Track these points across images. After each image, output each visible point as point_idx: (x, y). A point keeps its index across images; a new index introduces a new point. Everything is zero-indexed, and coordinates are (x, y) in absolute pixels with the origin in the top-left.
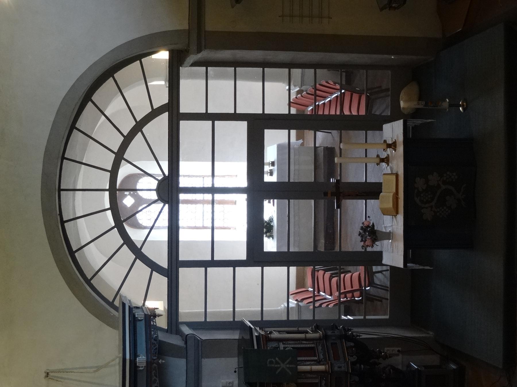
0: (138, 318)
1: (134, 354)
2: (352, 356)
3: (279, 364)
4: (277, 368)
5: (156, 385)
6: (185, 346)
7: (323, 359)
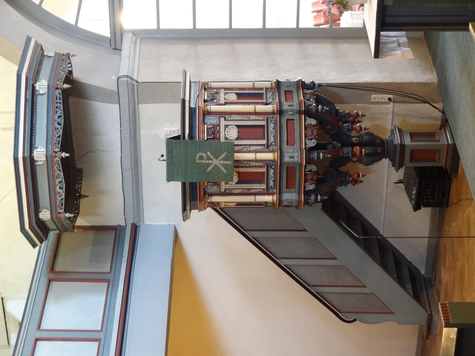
0: (39, 91)
1: (32, 147)
2: (311, 140)
3: (211, 159)
4: (209, 165)
5: (60, 180)
7: (273, 142)
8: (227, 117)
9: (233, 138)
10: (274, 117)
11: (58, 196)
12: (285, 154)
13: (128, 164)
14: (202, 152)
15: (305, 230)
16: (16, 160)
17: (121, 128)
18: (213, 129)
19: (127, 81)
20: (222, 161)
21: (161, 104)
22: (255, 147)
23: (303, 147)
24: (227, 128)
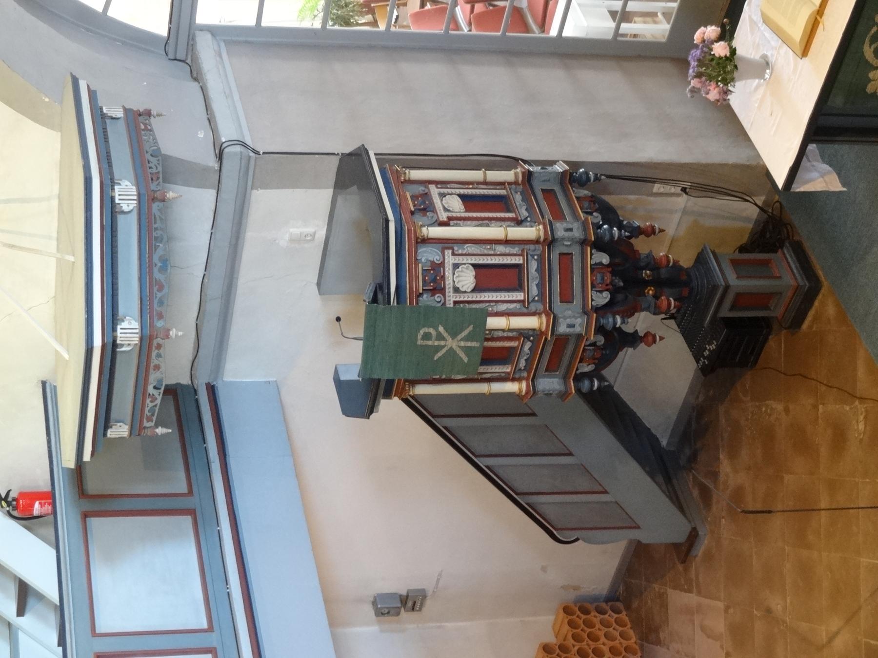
0: (121, 205)
1: (112, 318)
2: (601, 292)
3: (444, 339)
4: (438, 348)
6: (217, 166)
7: (536, 296)
8: (456, 248)
9: (468, 288)
10: (537, 248)
11: (148, 401)
12: (561, 320)
13: (215, 289)
14: (429, 327)
15: (534, 415)
16: (89, 350)
17: (212, 229)
18: (433, 273)
19: (241, 152)
20: (462, 342)
21: (293, 190)
22: (505, 304)
23: (589, 306)
24: (458, 270)
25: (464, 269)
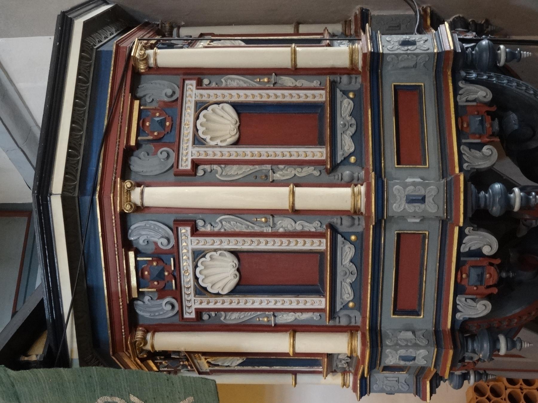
25: (205, 272)
